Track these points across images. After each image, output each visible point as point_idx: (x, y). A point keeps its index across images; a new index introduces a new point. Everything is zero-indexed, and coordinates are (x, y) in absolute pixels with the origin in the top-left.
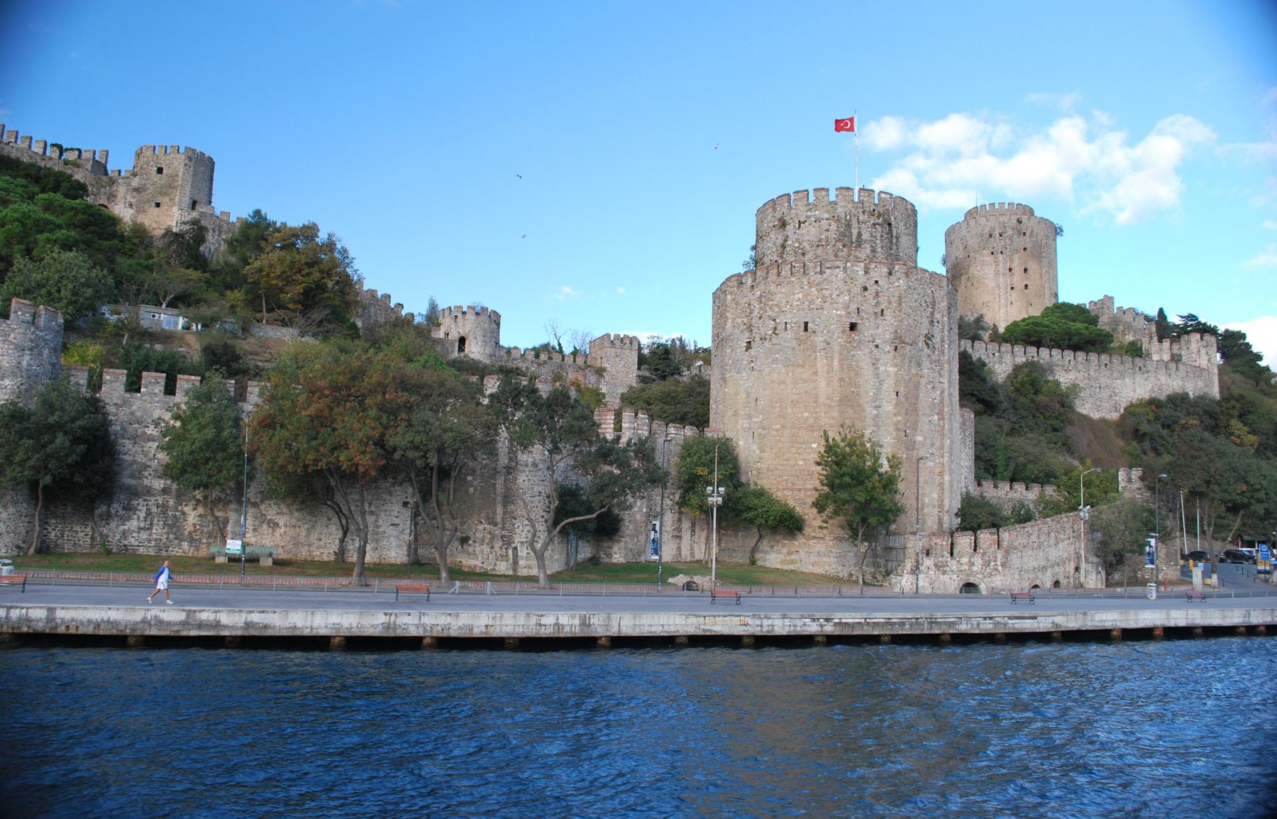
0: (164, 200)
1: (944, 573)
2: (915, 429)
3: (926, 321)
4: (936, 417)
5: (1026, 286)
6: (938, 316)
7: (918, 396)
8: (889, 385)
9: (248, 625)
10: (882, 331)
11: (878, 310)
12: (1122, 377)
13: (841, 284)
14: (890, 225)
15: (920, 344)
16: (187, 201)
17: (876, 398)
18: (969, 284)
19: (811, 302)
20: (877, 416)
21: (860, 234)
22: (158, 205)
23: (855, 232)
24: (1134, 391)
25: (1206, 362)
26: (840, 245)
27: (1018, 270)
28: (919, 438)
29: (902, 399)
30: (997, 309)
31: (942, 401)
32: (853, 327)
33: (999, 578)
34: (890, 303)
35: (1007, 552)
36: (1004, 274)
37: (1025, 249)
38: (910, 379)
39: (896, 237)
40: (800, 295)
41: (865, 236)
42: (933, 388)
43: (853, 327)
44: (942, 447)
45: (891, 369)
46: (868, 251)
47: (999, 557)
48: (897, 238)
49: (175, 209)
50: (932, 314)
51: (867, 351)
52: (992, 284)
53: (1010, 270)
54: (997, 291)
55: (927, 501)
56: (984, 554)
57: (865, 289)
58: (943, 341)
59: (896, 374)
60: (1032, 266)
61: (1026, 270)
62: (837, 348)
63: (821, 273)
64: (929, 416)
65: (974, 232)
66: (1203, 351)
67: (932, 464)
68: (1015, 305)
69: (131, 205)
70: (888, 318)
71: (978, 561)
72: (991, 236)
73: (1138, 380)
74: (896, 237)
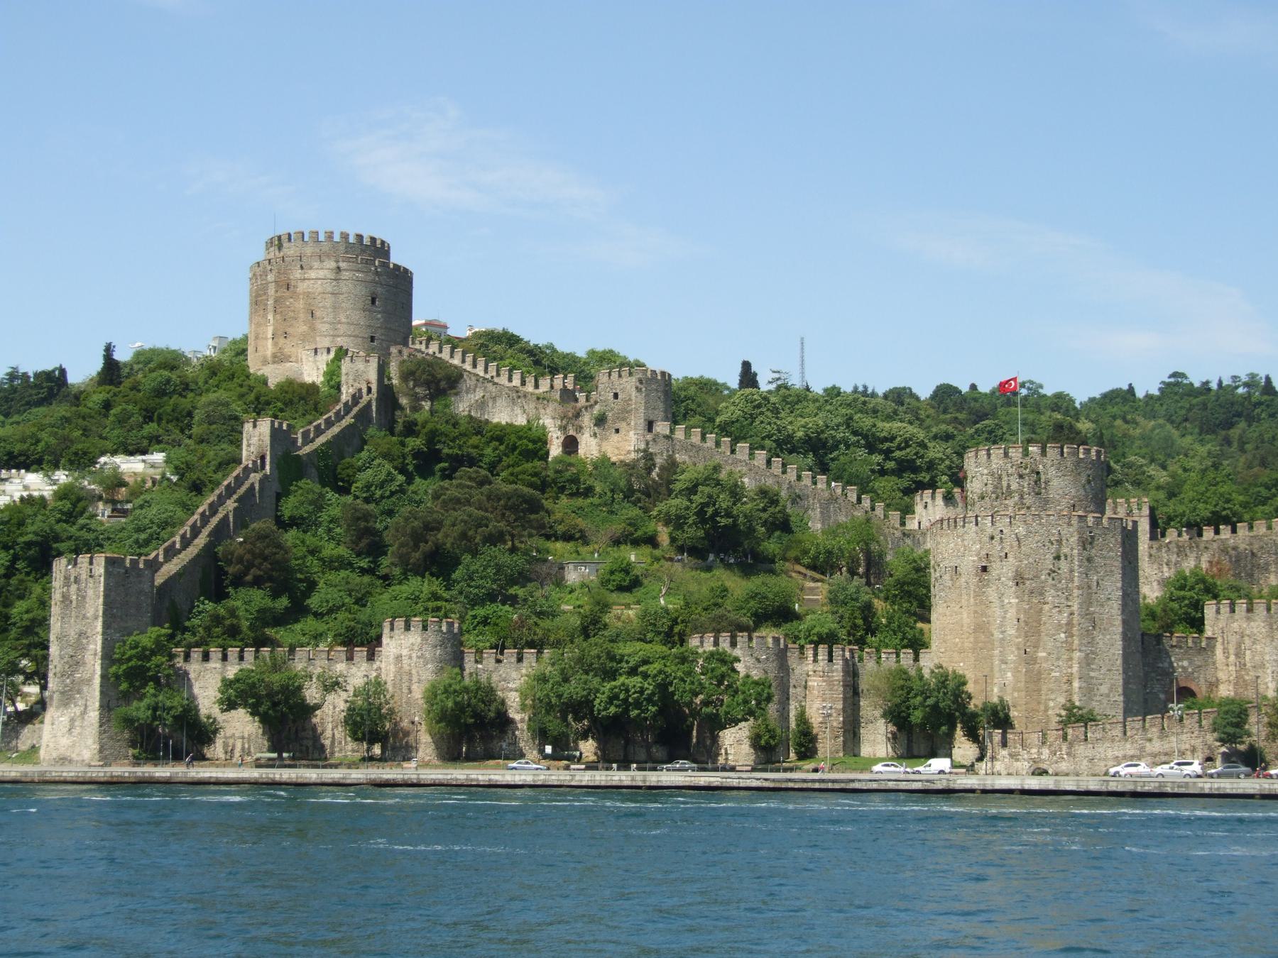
0: (622, 425)
1: (1017, 760)
2: (1036, 647)
3: (1050, 557)
4: (1063, 635)
6: (1065, 550)
7: (1040, 620)
8: (1012, 613)
9: (490, 780)
10: (1003, 571)
11: (1003, 554)
13: (974, 535)
14: (1038, 473)
15: (1043, 577)
16: (641, 422)
17: (1001, 625)
19: (959, 551)
20: (1003, 639)
21: (1009, 486)
22: (617, 431)
23: (1005, 484)
26: (994, 496)
28: (1042, 654)
29: (1022, 624)
31: (1070, 624)
32: (984, 569)
33: (1064, 764)
34: (1012, 547)
35: (1071, 745)
38: (1030, 608)
39: (1045, 483)
40: (952, 545)
42: (1060, 611)
43: (984, 569)
44: (1071, 659)
45: (1013, 601)
46: (1016, 498)
47: (1064, 748)
49: (632, 433)
50: (1058, 550)
51: (994, 587)
55: (1051, 704)
56: (1050, 746)
57: (992, 538)
58: (1072, 571)
59: (1017, 604)
62: (972, 588)
63: (964, 526)
64: (1054, 635)
67: (1058, 674)
69: (595, 435)
70: (1011, 558)
71: (1046, 752)
74: (1045, 483)
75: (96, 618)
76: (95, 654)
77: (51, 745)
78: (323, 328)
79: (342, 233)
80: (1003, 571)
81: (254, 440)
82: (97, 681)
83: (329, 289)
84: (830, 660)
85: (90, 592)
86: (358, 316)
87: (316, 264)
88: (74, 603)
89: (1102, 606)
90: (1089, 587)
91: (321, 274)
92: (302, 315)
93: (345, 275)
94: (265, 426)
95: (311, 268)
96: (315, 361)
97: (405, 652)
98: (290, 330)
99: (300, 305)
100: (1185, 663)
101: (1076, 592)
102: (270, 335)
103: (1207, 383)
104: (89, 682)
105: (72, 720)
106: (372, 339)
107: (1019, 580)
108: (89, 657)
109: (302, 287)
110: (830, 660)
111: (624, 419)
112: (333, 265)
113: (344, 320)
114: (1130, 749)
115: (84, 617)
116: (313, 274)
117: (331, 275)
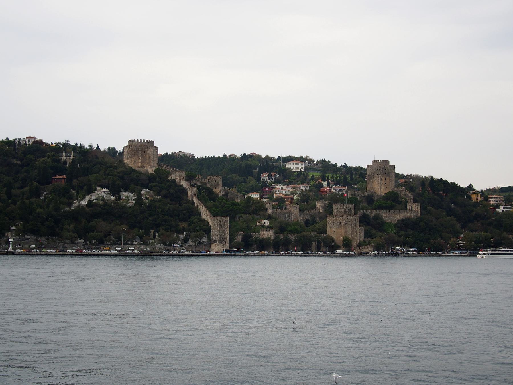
2: (353, 235)
5: (386, 183)
10: (349, 224)
12: (397, 214)
18: (372, 182)
22: (215, 188)
25: (417, 209)
27: (384, 179)
30: (378, 189)
31: (357, 232)
35: (363, 249)
36: (380, 180)
37: (386, 174)
41: (348, 211)
43: (346, 223)
45: (351, 228)
52: (377, 183)
53: (382, 179)
54: (378, 184)
60: (387, 178)
61: (386, 179)
65: (373, 168)
66: (416, 207)
68: (383, 188)
72: (377, 170)
75: (227, 228)
76: (227, 234)
77: (219, 250)
79: (143, 140)
80: (349, 224)
81: (193, 191)
82: (228, 238)
83: (153, 153)
85: (226, 223)
88: (222, 225)
91: (151, 150)
92: (148, 158)
95: (149, 149)
96: (152, 169)
97: (270, 234)
98: (145, 161)
99: (147, 156)
102: (140, 162)
103: (76, 144)
104: (226, 239)
105: (223, 245)
107: (351, 225)
108: (226, 235)
109: (148, 152)
111: (217, 186)
112: (153, 148)
115: (225, 228)
116: (150, 150)
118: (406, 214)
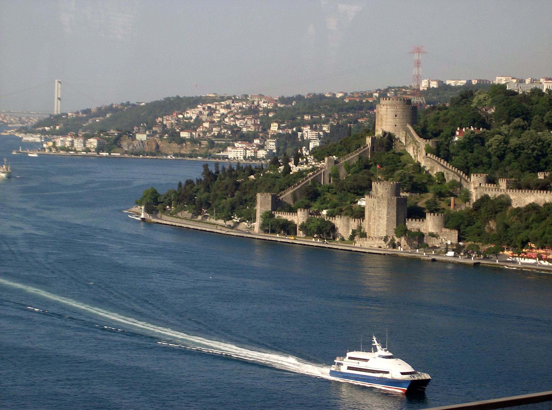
2: (370, 222)
24: (530, 200)
28: (371, 223)
48: (377, 190)
73: (532, 197)
78: (384, 123)
84: (355, 221)
86: (391, 120)
87: (383, 107)
89: (382, 215)
90: (379, 211)
93: (389, 110)
94: (327, 158)
100: (418, 225)
101: (376, 212)
106: (396, 126)
109: (380, 113)
110: (355, 221)
113: (388, 121)
114: (373, 242)
116: (382, 110)
117: (386, 110)
118: (539, 196)
